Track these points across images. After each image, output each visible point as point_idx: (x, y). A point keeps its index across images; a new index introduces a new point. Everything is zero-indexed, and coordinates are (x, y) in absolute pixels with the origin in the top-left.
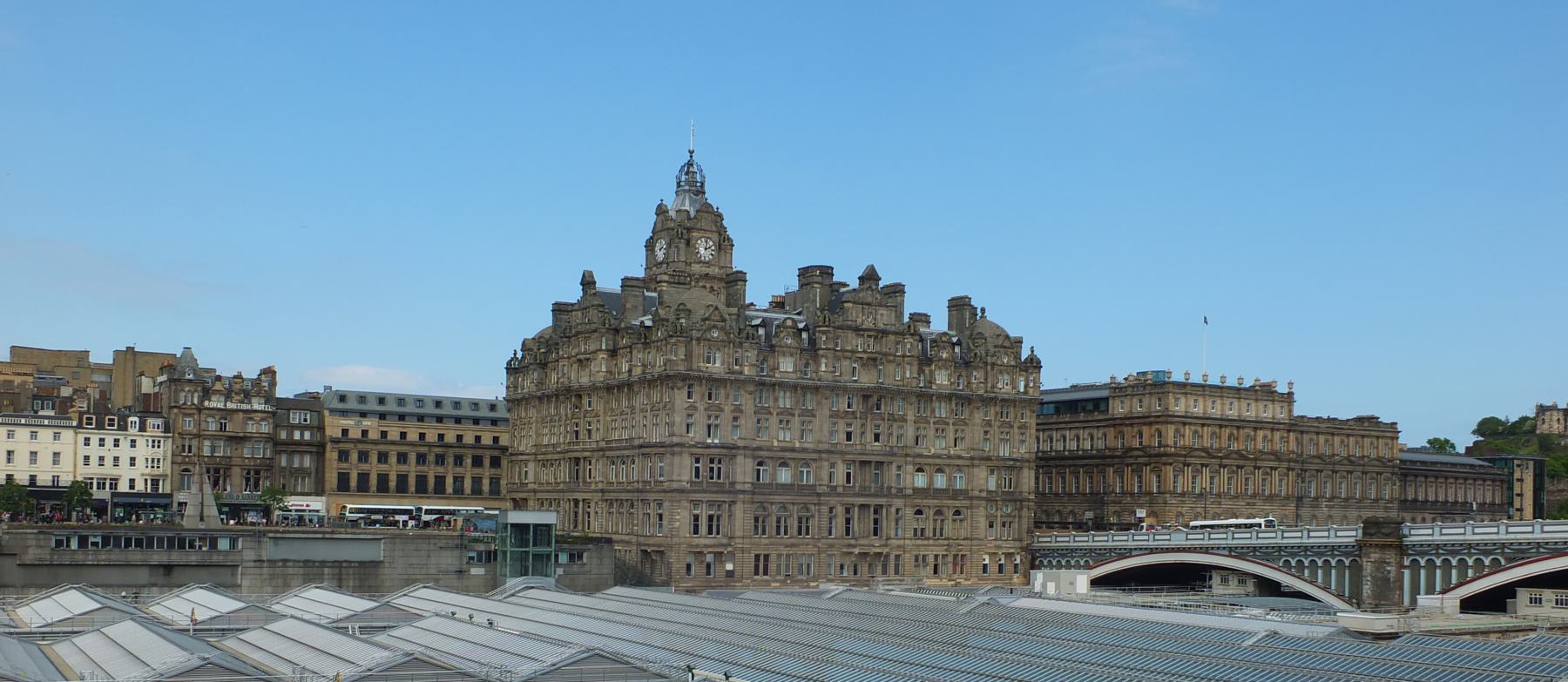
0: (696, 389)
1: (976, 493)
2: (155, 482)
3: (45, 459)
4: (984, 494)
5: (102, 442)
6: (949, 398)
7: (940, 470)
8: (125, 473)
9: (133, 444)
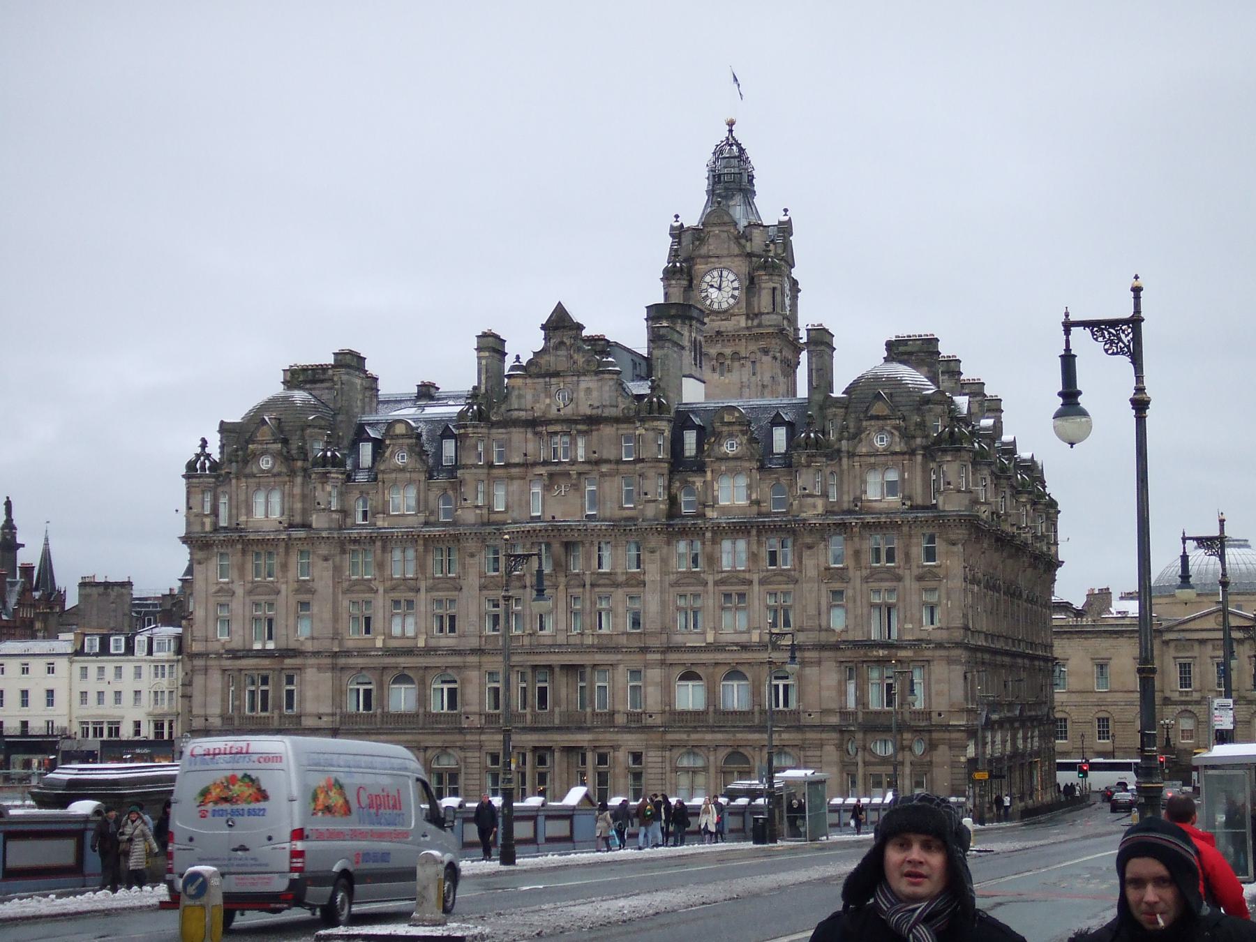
1: (815, 719)
2: (159, 726)
3: (38, 698)
4: (834, 720)
6: (740, 529)
7: (734, 674)
9: (138, 674)
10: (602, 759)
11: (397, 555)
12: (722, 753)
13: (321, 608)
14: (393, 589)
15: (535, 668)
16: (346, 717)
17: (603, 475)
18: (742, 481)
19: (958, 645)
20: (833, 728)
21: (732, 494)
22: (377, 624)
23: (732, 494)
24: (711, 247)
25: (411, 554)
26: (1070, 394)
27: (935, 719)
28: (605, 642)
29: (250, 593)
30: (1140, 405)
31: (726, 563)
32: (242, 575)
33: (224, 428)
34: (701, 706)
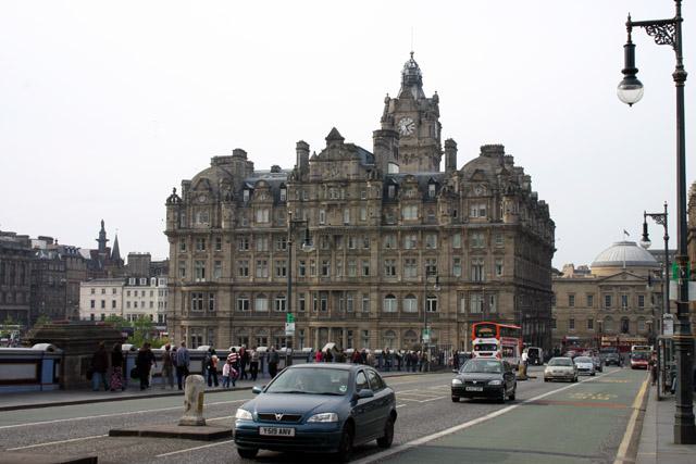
0: (188, 242)
1: (446, 316)
2: (160, 317)
3: (109, 304)
4: (456, 317)
5: (104, 292)
6: (414, 231)
8: (147, 311)
9: (152, 293)
10: (350, 333)
11: (260, 241)
12: (405, 331)
13: (226, 264)
14: (258, 256)
15: (320, 292)
16: (236, 313)
17: (352, 205)
18: (415, 209)
19: (510, 284)
20: (454, 321)
21: (411, 214)
22: (251, 271)
23: (411, 214)
24: (404, 107)
25: (266, 241)
26: (630, 72)
27: (501, 317)
28: (352, 280)
29: (195, 256)
30: (680, 77)
31: (408, 246)
32: (191, 250)
33: (186, 184)
34: (394, 311)
